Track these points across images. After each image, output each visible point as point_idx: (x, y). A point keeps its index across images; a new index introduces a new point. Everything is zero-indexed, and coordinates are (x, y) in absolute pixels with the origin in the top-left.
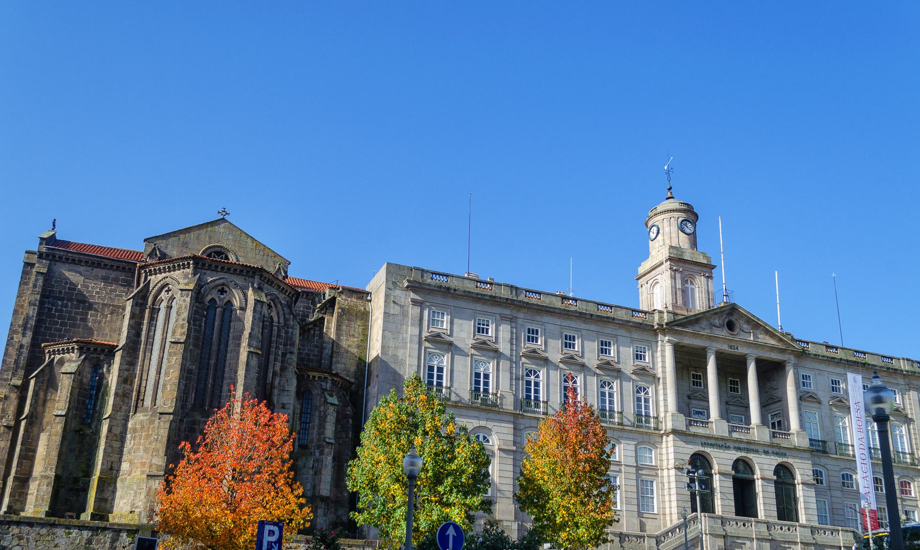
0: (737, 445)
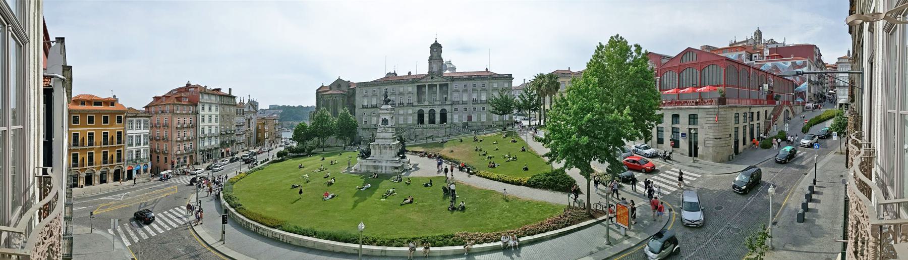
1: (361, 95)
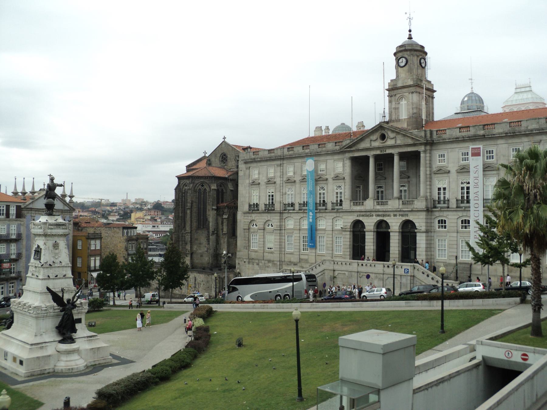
0: (377, 213)
1: (247, 181)
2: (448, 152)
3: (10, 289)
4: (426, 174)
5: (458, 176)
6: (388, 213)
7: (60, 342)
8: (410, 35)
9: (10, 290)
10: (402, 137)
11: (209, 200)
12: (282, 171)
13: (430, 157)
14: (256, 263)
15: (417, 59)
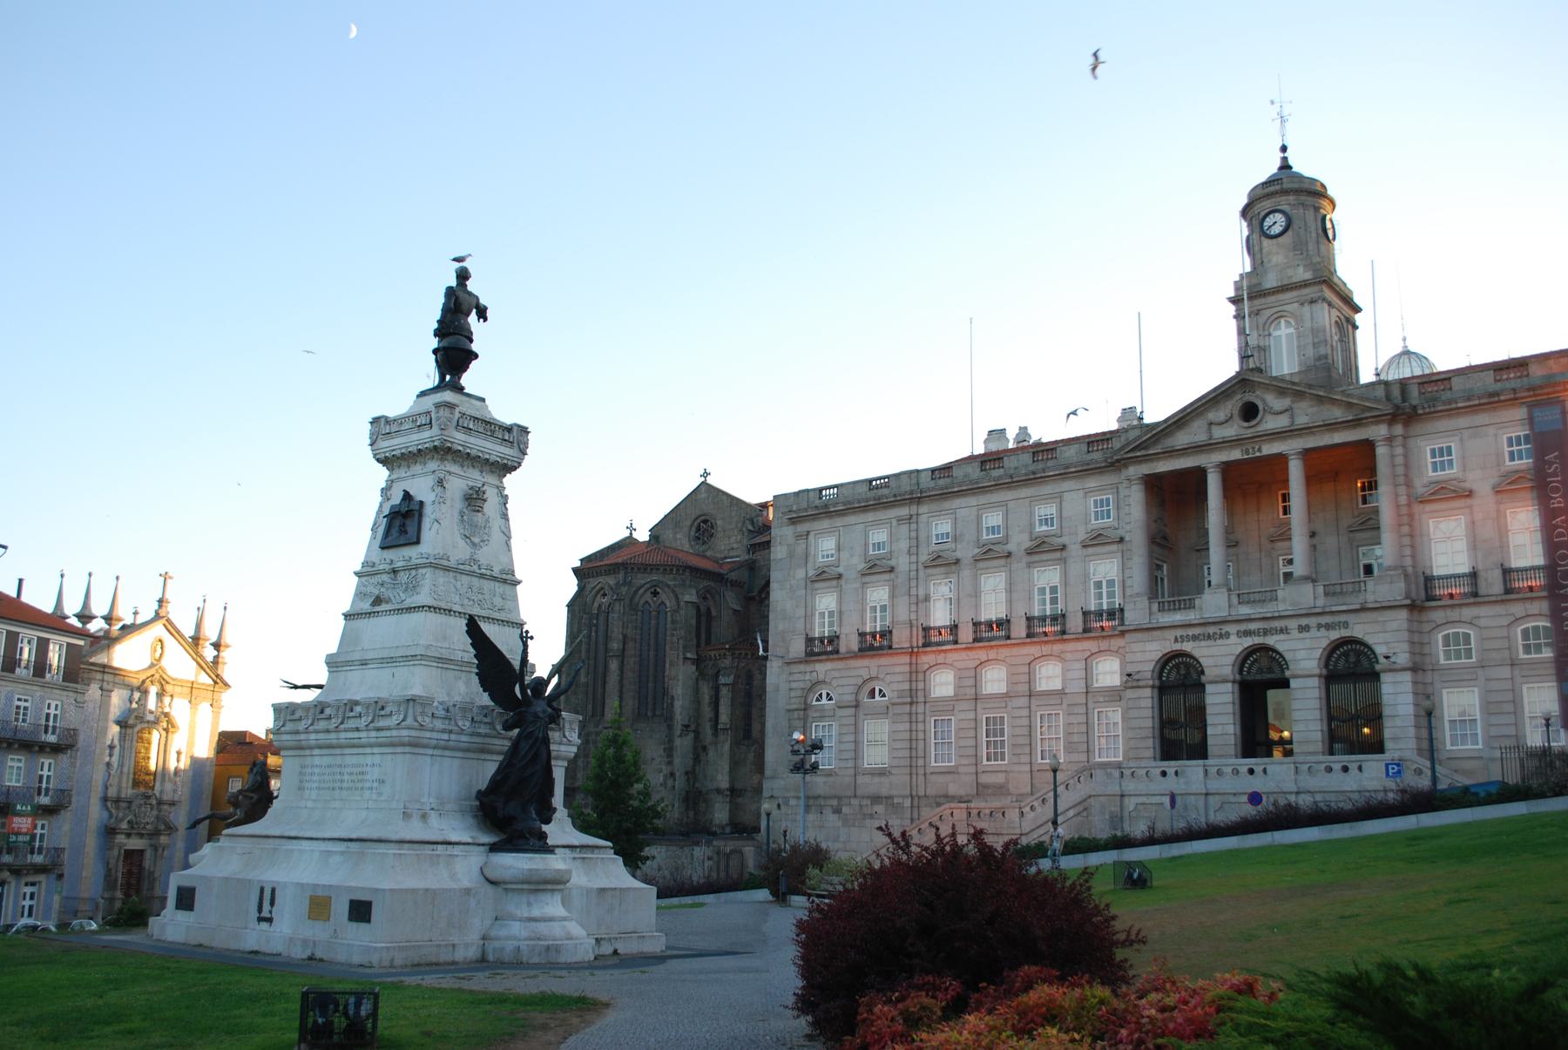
1: (800, 574)
2: (1461, 440)
3: (24, 903)
4: (1398, 506)
5: (1499, 503)
6: (1277, 624)
7: (494, 848)
8: (1285, 159)
9: (24, 907)
10: (1312, 406)
11: (673, 635)
12: (913, 534)
13: (1406, 456)
14: (832, 806)
15: (1316, 216)
